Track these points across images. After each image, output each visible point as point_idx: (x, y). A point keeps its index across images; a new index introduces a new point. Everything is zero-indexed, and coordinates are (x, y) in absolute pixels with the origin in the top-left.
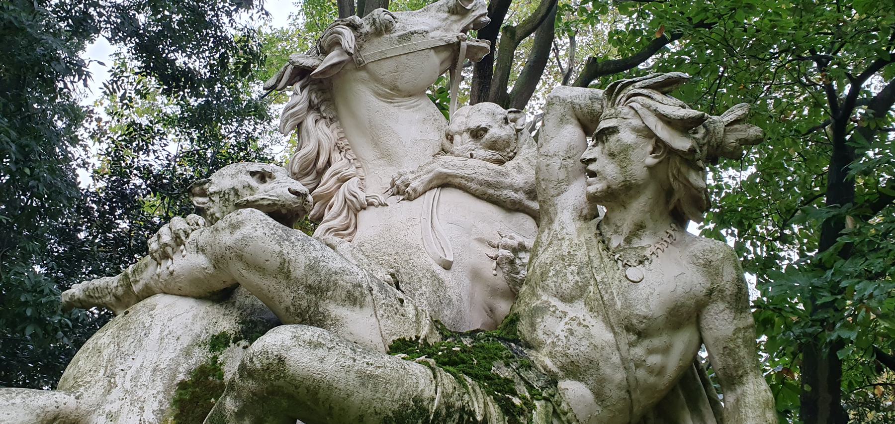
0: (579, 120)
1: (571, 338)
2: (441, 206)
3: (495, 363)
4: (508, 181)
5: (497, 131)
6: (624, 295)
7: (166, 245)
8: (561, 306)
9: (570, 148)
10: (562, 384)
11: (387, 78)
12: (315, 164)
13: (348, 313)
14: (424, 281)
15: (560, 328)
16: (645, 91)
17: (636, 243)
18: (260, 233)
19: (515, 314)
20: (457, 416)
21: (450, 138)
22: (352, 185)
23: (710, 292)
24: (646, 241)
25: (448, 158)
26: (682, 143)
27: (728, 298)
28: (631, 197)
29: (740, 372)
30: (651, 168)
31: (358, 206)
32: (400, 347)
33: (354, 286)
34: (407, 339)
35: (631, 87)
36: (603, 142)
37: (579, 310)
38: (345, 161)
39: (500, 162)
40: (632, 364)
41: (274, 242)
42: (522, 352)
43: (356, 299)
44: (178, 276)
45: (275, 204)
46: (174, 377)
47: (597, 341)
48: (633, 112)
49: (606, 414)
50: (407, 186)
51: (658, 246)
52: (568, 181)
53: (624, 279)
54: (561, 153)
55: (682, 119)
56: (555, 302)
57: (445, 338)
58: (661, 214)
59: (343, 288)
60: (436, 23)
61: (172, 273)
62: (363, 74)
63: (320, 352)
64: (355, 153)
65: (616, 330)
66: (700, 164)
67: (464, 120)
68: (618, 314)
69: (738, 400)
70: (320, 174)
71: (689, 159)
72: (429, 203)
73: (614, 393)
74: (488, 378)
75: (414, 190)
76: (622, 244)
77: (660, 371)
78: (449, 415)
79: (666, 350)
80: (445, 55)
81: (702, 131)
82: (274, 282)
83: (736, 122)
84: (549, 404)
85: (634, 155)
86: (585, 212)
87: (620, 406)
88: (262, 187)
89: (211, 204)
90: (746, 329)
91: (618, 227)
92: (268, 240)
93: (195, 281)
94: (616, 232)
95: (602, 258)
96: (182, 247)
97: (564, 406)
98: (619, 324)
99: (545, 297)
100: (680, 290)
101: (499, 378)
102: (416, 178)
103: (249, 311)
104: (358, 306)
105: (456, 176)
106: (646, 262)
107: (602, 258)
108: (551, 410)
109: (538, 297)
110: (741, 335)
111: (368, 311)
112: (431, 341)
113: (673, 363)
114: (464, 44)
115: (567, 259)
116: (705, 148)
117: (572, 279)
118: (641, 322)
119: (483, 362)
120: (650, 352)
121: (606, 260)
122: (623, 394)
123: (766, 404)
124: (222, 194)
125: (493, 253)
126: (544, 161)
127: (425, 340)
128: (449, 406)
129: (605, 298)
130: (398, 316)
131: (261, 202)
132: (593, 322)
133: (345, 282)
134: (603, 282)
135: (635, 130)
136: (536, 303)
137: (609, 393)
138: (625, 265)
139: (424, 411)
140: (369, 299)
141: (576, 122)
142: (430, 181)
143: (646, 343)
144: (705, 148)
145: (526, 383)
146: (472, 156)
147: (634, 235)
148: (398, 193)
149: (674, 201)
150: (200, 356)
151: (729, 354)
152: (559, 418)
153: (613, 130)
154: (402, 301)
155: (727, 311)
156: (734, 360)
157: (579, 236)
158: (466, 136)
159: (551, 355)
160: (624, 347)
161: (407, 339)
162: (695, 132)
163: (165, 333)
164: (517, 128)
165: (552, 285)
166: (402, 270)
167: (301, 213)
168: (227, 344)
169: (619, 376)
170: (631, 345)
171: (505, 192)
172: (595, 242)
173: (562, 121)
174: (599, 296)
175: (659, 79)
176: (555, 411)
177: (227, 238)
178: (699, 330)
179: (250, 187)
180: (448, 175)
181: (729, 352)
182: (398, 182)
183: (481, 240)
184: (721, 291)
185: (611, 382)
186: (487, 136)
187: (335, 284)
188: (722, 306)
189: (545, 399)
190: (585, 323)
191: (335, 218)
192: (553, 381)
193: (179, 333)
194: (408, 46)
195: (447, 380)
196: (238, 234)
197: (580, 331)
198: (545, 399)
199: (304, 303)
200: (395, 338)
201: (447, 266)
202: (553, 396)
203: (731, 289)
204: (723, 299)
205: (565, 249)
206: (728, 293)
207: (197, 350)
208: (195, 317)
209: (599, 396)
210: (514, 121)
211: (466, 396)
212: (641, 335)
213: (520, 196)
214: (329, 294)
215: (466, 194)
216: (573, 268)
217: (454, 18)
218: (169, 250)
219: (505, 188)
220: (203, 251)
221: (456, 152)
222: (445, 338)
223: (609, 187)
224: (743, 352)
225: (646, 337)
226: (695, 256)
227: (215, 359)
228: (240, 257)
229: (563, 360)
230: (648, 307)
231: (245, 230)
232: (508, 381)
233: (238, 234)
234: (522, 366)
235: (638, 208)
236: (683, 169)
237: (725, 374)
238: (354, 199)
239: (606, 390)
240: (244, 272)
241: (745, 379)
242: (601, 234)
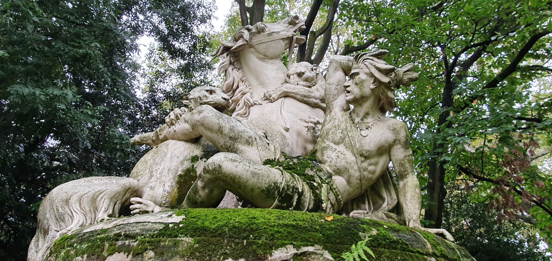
0: (343, 69)
1: (338, 159)
2: (285, 105)
3: (307, 169)
4: (313, 95)
5: (308, 74)
6: (360, 142)
7: (173, 119)
8: (334, 146)
9: (339, 81)
10: (333, 177)
11: (262, 51)
12: (232, 87)
13: (247, 148)
14: (278, 136)
15: (333, 155)
17: (365, 120)
18: (210, 115)
19: (315, 150)
20: (291, 190)
21: (289, 76)
22: (248, 96)
24: (369, 120)
25: (288, 85)
26: (385, 79)
27: (402, 143)
28: (364, 102)
29: (406, 173)
30: (372, 90)
31: (250, 105)
32: (268, 162)
33: (249, 137)
34: (271, 159)
35: (365, 56)
36: (353, 79)
37: (341, 148)
38: (245, 86)
39: (310, 87)
40: (362, 170)
41: (216, 119)
42: (318, 165)
43: (250, 143)
44: (178, 132)
45: (216, 104)
47: (349, 161)
48: (365, 66)
49: (351, 189)
50: (271, 96)
51: (374, 122)
52: (338, 95)
53: (360, 135)
54: (335, 83)
55: (386, 69)
56: (332, 145)
57: (286, 159)
58: (376, 109)
59: (244, 138)
60: (283, 28)
61: (175, 131)
62: (252, 49)
63: (236, 163)
64: (249, 82)
65: (356, 156)
66: (393, 88)
67: (295, 69)
68: (357, 149)
69: (405, 184)
70: (234, 91)
71: (388, 86)
72: (279, 104)
73: (355, 181)
74: (304, 175)
75: (273, 98)
76: (360, 121)
77: (373, 172)
78: (288, 189)
79: (376, 164)
80: (287, 42)
81: (393, 74)
82: (216, 135)
83: (408, 71)
84: (328, 185)
85: (365, 84)
86: (345, 108)
87: (357, 186)
88: (211, 96)
89: (190, 103)
90: (409, 156)
91: (358, 114)
93: (185, 134)
94: (357, 116)
95: (351, 127)
96: (179, 120)
97: (334, 186)
98: (358, 154)
99: (327, 143)
100: (383, 140)
101: (308, 175)
102: (274, 93)
103: (206, 147)
105: (291, 93)
106: (369, 129)
107: (351, 127)
108: (329, 188)
109: (325, 143)
110: (407, 158)
111: (255, 148)
112: (281, 160)
113: (379, 169)
114: (295, 37)
115: (337, 127)
116: (395, 81)
117: (339, 135)
118: (367, 153)
119: (302, 169)
120: (370, 165)
121: (353, 127)
122: (359, 182)
123: (416, 186)
124: (195, 99)
125: (306, 125)
126: (328, 86)
127: (278, 160)
128: (288, 186)
129: (352, 143)
130: (267, 150)
131: (210, 103)
132: (347, 152)
133: (245, 135)
134: (351, 137)
135: (366, 74)
136: (324, 145)
138: (361, 130)
139: (278, 188)
140: (255, 143)
141: (342, 70)
142: (280, 95)
143: (368, 161)
144: (395, 81)
145: (319, 177)
146: (298, 84)
147: (365, 117)
148: (267, 99)
149: (381, 103)
150: (187, 165)
151: (402, 166)
152: (332, 191)
153: (357, 74)
154: (268, 144)
155: (402, 148)
156: (404, 168)
157: (342, 118)
158: (296, 76)
159: (330, 166)
160: (359, 163)
161: (271, 159)
162: (391, 75)
163: (173, 155)
164: (317, 72)
165: (331, 138)
166: (268, 132)
167: (227, 107)
168: (198, 160)
169: (357, 174)
170: (362, 162)
171: (312, 99)
172: (349, 120)
173: (336, 70)
174: (350, 142)
175: (377, 52)
176: (331, 188)
177: (197, 117)
178: (390, 156)
179: (206, 96)
180: (288, 92)
181: (402, 165)
182: (267, 95)
183: (301, 120)
184: (399, 140)
185: (354, 177)
186: (304, 76)
188: (399, 146)
189: (327, 183)
190: (344, 153)
191: (240, 110)
192: (330, 176)
193: (178, 155)
194: (272, 38)
195: (287, 175)
196: (201, 115)
197: (341, 156)
198: (327, 183)
200: (266, 159)
201: (287, 130)
202: (330, 182)
204: (400, 144)
205: (336, 123)
206: (402, 141)
207: (186, 162)
208: (185, 149)
209: (349, 182)
210: (316, 70)
211: (295, 182)
212: (366, 158)
213: (318, 101)
214: (239, 140)
215: (295, 100)
216: (339, 131)
217: (291, 26)
218: (174, 122)
219: (312, 98)
220: (187, 122)
221: (291, 83)
222: (286, 159)
223: (355, 97)
224: (407, 165)
225: (368, 159)
226: (389, 126)
227: (193, 165)
228: (203, 125)
229: (335, 168)
230: (369, 146)
232: (312, 176)
233: (201, 115)
234: (318, 170)
235: (367, 106)
236: (386, 90)
237: (400, 174)
238: (248, 102)
239: (352, 180)
240: (204, 131)
241: (408, 176)
242: (351, 117)
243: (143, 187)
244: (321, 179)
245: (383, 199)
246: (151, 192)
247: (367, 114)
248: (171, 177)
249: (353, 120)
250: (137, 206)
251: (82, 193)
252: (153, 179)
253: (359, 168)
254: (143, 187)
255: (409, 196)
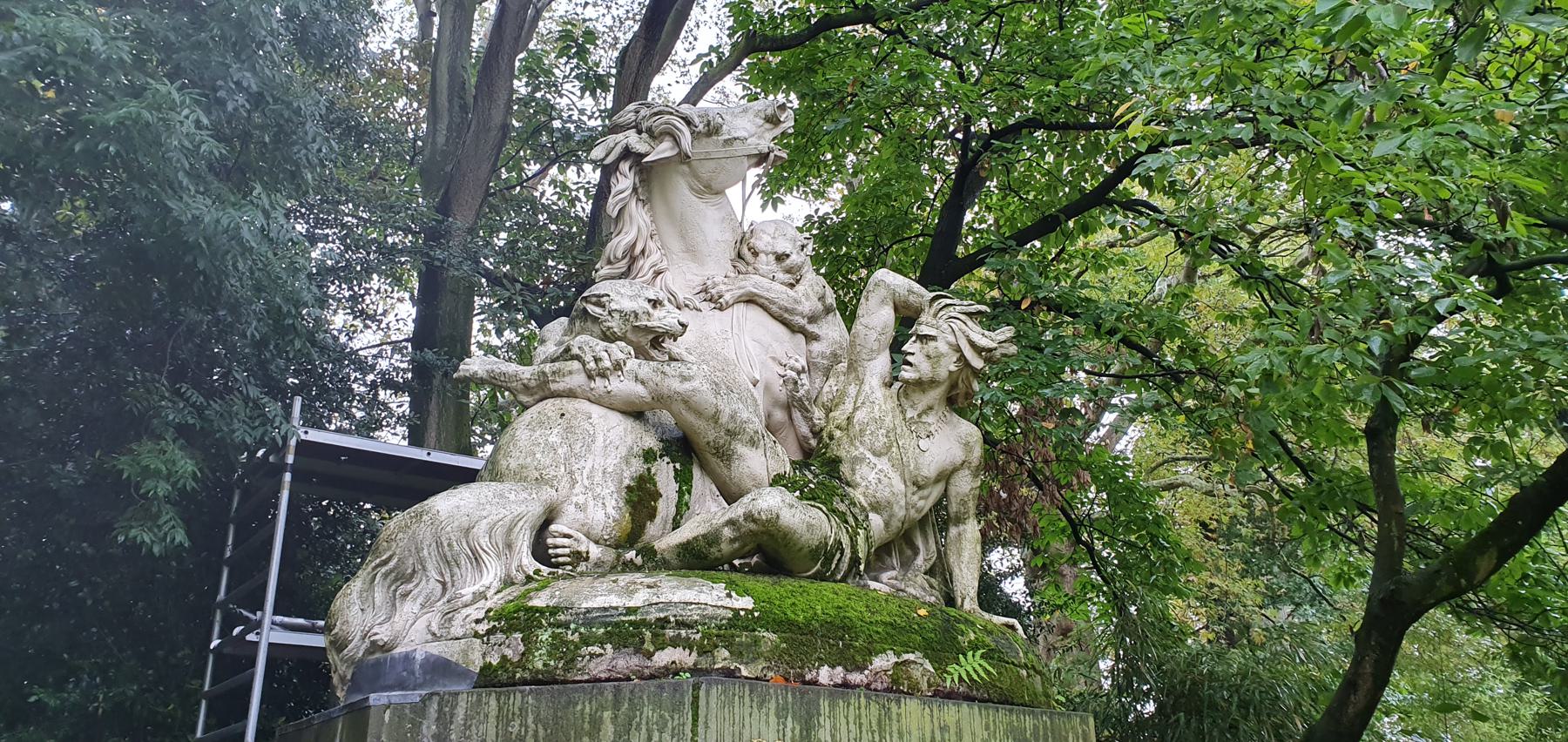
8: (874, 459)
15: (872, 476)
16: (963, 317)
17: (924, 418)
18: (705, 388)
24: (930, 419)
26: (977, 363)
37: (883, 464)
39: (792, 286)
46: (621, 483)
50: (720, 297)
56: (869, 455)
73: (895, 524)
85: (943, 361)
92: (709, 393)
99: (861, 450)
100: (948, 462)
115: (879, 421)
120: (921, 498)
135: (949, 344)
150: (638, 466)
158: (772, 258)
168: (655, 459)
169: (901, 513)
180: (756, 295)
183: (774, 359)
196: (687, 386)
197: (885, 481)
199: (722, 441)
207: (633, 460)
209: (887, 525)
212: (920, 488)
213: (803, 322)
227: (649, 469)
228: (686, 402)
231: (695, 384)
233: (687, 386)
235: (935, 395)
243: (562, 502)
244: (856, 519)
245: (916, 552)
246: (581, 516)
247: (931, 408)
248: (613, 489)
249: (903, 412)
250: (560, 541)
251: (496, 518)
252: (578, 489)
253: (907, 503)
254: (562, 502)
255: (966, 555)
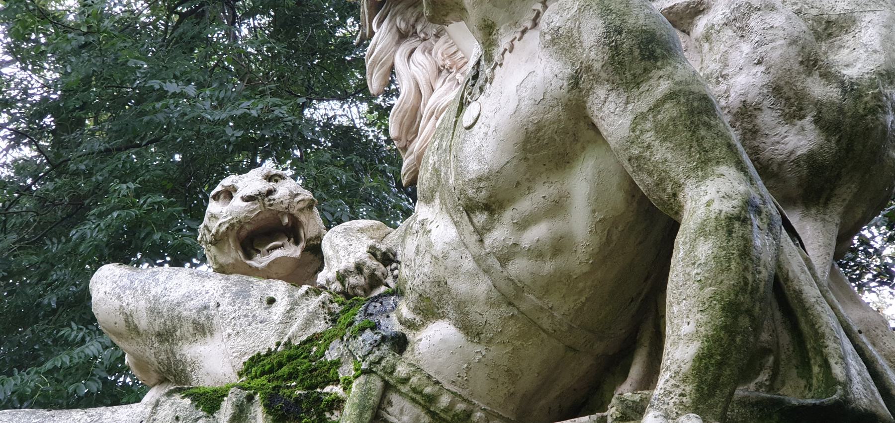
13: (202, 348)
23: (575, 82)
27: (603, 75)
43: (203, 328)
104: (208, 335)
110: (648, 125)
120: (523, 225)
133: (189, 311)
137: (480, 320)
143: (508, 215)
155: (613, 96)
156: (650, 174)
169: (482, 287)
184: (589, 69)
187: (179, 318)
203: (600, 56)
204: (597, 79)
206: (597, 66)
214: (178, 333)
239: (473, 316)
